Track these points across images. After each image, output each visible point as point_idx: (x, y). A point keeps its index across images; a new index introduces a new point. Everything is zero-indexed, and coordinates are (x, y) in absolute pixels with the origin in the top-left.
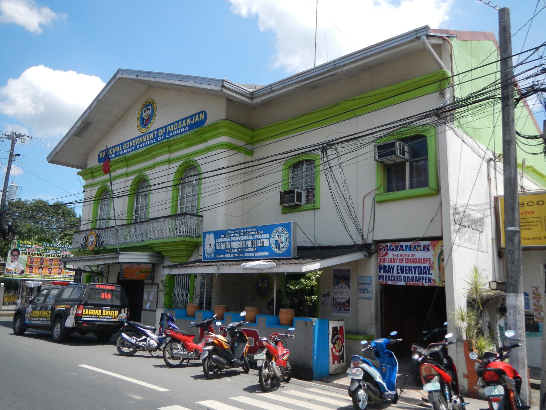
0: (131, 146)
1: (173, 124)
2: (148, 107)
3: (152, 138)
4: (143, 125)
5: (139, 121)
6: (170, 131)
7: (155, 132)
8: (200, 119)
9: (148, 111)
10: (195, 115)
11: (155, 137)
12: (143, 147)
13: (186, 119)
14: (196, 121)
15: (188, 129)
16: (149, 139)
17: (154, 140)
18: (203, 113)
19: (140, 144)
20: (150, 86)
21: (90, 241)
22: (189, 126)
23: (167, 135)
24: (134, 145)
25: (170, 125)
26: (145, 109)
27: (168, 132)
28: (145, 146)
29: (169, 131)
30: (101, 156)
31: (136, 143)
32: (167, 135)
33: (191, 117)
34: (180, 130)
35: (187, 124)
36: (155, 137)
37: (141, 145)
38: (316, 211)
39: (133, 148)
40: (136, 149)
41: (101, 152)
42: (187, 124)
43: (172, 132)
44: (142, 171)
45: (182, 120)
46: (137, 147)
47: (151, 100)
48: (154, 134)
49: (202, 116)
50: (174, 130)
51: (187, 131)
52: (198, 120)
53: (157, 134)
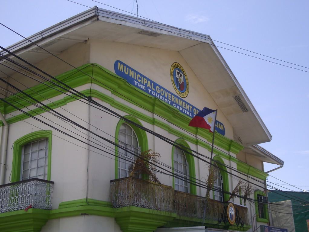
2: (181, 74)
3: (188, 110)
4: (178, 87)
5: (172, 78)
11: (191, 111)
20: (178, 52)
21: (230, 214)
26: (178, 71)
30: (121, 67)
36: (191, 111)
39: (170, 102)
41: (122, 63)
44: (184, 138)
46: (174, 104)
47: (174, 64)
49: (222, 128)
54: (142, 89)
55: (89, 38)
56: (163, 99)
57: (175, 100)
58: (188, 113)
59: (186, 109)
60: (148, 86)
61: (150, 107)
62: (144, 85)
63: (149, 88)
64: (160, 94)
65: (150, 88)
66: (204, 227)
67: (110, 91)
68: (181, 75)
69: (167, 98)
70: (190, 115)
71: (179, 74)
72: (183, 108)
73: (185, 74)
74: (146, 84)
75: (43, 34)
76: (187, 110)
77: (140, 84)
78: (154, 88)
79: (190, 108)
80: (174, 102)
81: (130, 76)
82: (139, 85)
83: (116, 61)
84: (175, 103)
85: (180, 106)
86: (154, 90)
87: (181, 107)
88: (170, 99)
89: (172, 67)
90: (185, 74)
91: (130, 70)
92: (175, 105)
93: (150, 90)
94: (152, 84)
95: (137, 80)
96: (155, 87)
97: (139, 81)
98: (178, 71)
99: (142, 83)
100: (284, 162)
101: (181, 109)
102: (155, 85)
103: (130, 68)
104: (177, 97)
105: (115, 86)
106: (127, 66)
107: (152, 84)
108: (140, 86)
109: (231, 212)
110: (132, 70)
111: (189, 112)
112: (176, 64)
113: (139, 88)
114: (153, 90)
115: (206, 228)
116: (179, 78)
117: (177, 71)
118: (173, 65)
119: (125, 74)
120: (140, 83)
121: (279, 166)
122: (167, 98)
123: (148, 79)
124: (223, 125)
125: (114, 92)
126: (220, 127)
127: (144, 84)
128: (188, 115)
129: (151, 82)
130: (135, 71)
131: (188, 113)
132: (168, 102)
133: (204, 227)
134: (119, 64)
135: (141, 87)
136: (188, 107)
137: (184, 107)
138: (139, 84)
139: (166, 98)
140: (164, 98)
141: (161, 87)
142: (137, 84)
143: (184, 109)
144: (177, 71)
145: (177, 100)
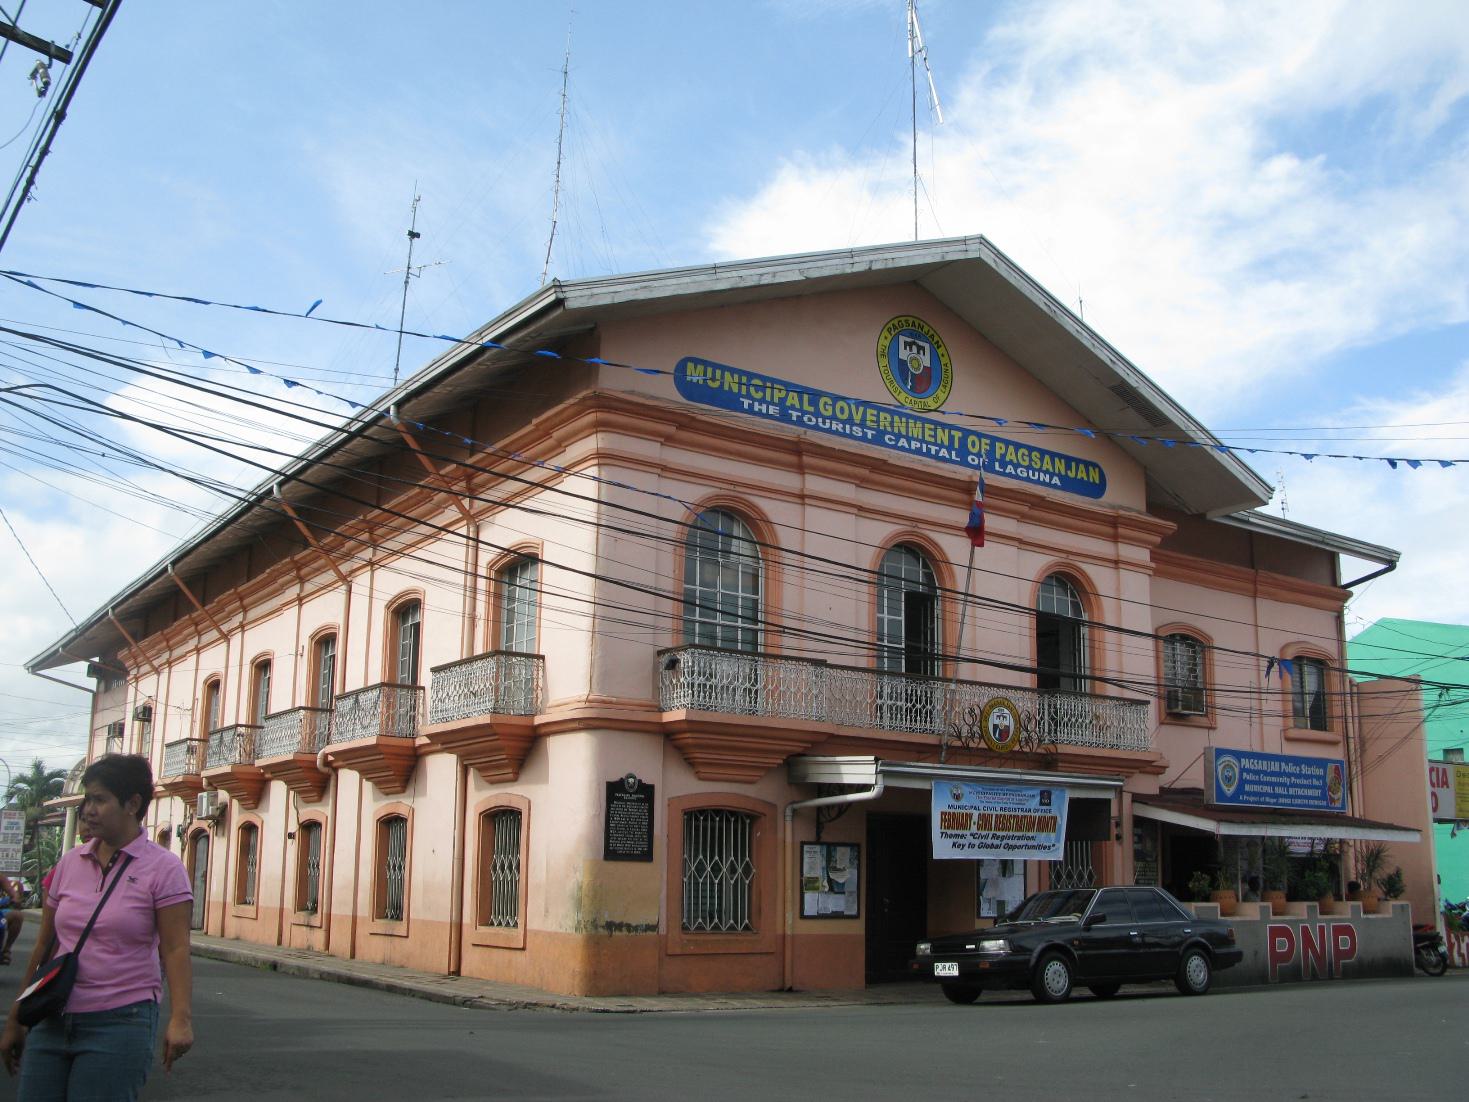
0: (857, 418)
1: (1018, 446)
2: (921, 343)
3: (946, 443)
4: (906, 384)
5: (884, 362)
6: (1007, 459)
7: (957, 435)
8: (1091, 480)
9: (918, 353)
10: (1078, 461)
11: (956, 446)
12: (909, 451)
13: (1053, 455)
14: (1079, 477)
15: (1059, 484)
16: (933, 440)
17: (953, 453)
18: (1097, 470)
19: (899, 436)
20: (915, 282)
21: (995, 727)
22: (1059, 475)
23: (997, 464)
24: (869, 423)
25: (1007, 443)
26: (909, 340)
27: (998, 456)
28: (918, 451)
29: (1003, 456)
30: (695, 374)
31: (878, 422)
32: (997, 464)
33: (1068, 460)
34: (1037, 474)
35: (1057, 471)
36: (956, 446)
37: (903, 442)
38: (1211, 731)
40: (878, 440)
41: (697, 361)
42: (1057, 471)
43: (1016, 466)
45: (1043, 453)
46: (887, 437)
48: (951, 438)
49: (1094, 477)
50: (1020, 466)
51: (1055, 486)
52: (1085, 479)
53: (963, 441)
54: (767, 416)
55: (596, 324)
56: (844, 428)
57: (892, 423)
58: (943, 453)
59: (935, 444)
60: (788, 403)
61: (792, 459)
62: (774, 404)
63: (793, 407)
64: (833, 418)
65: (798, 406)
66: (872, 758)
67: (657, 441)
68: (920, 348)
69: (863, 424)
70: (954, 457)
71: (915, 348)
72: (922, 441)
73: (938, 342)
74: (783, 400)
75: (483, 335)
76: (941, 446)
77: (760, 404)
78: (810, 404)
79: (951, 438)
80: (889, 429)
81: (726, 388)
82: (757, 407)
83: (677, 366)
84: (892, 433)
85: (909, 439)
86: (811, 409)
87: (917, 440)
88: (875, 425)
89: (885, 333)
90: (938, 342)
91: (727, 375)
92: (890, 439)
93: (795, 415)
94: (806, 397)
95: (749, 396)
96: (814, 402)
97: (759, 395)
98: (909, 340)
99: (768, 398)
100: (1399, 554)
101: (914, 445)
102: (815, 396)
103: (724, 368)
104: (901, 415)
105: (671, 429)
106: (715, 366)
107: (806, 397)
108: (760, 410)
109: (997, 722)
110: (733, 371)
111: (950, 448)
112: (903, 319)
113: (759, 414)
114: (805, 413)
115: (876, 760)
116: (912, 359)
117: (902, 339)
118: (890, 325)
119: (712, 388)
120: (762, 401)
121: (1381, 567)
122: (863, 424)
123: (789, 387)
124: (1095, 465)
125: (668, 440)
126: (1082, 475)
127: (776, 400)
128: (943, 460)
129: (801, 391)
130: (742, 373)
131: (943, 453)
132: (865, 434)
133: (872, 758)
134: (690, 366)
135: (764, 411)
136: (943, 436)
137: (927, 438)
138: (756, 404)
139: (857, 425)
140: (848, 427)
141: (836, 398)
142: (751, 406)
143: (928, 443)
144: (902, 339)
145: (900, 425)
